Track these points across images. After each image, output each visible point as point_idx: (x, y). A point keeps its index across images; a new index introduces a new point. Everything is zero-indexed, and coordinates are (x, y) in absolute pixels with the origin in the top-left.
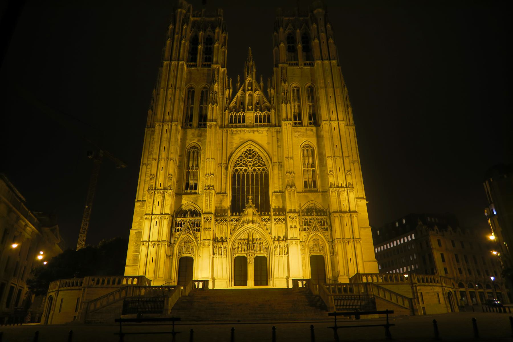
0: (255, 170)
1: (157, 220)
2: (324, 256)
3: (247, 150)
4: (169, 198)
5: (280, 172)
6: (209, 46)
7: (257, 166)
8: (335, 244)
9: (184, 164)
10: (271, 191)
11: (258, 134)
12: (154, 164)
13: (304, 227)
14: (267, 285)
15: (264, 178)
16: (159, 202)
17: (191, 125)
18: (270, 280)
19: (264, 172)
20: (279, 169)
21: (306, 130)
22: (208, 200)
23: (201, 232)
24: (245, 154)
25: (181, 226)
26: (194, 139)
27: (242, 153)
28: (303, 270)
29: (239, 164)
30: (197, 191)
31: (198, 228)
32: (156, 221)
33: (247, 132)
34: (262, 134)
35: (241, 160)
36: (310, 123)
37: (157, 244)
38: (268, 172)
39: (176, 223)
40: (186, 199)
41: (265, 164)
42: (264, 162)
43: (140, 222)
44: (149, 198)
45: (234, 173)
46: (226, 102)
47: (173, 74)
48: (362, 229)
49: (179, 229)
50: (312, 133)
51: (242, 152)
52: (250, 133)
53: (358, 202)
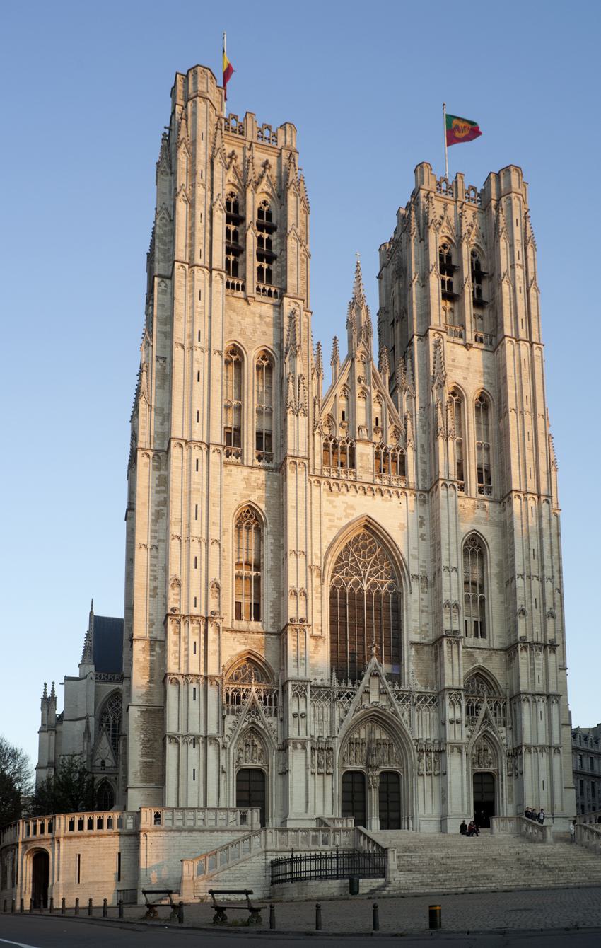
1: (195, 685)
3: (358, 535)
5: (423, 596)
8: (521, 753)
9: (231, 555)
11: (383, 500)
14: (399, 827)
17: (239, 455)
18: (408, 818)
25: (238, 703)
26: (249, 493)
38: (401, 593)
40: (242, 641)
46: (314, 407)
49: (236, 708)
51: (348, 541)
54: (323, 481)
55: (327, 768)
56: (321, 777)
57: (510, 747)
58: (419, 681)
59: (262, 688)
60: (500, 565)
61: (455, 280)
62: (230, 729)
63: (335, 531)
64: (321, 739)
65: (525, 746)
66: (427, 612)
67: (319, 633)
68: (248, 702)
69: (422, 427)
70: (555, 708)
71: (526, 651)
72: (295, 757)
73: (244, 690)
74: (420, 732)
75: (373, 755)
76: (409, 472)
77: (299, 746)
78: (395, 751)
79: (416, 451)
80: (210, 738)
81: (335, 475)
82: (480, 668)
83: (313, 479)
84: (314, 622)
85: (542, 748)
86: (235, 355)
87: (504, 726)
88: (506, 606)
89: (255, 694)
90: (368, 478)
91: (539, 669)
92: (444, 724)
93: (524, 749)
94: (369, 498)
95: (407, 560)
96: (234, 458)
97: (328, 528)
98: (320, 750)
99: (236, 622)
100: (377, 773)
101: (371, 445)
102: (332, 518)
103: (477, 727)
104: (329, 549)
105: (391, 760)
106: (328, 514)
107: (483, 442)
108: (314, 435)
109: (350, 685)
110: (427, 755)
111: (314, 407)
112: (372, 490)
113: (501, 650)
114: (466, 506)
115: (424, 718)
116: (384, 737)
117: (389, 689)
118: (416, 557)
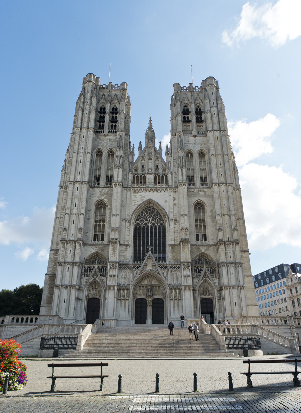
0: (154, 224)
2: (213, 300)
3: (147, 207)
4: (79, 247)
5: (175, 226)
6: (114, 115)
7: (156, 221)
10: (168, 242)
12: (67, 217)
13: (196, 274)
15: (162, 231)
16: (70, 250)
17: (98, 184)
19: (161, 227)
20: (174, 224)
21: (199, 190)
22: (113, 249)
23: (107, 278)
24: (145, 210)
25: (90, 272)
26: (101, 196)
27: (143, 210)
28: (195, 311)
29: (140, 219)
30: (103, 242)
31: (104, 273)
32: (68, 267)
33: (147, 191)
34: (161, 193)
35: (142, 215)
36: (202, 185)
37: (68, 288)
39: (85, 268)
40: (94, 248)
41: (162, 219)
42: (162, 217)
43: (54, 267)
44: (62, 247)
45: (136, 226)
46: (130, 165)
47: (83, 139)
48: (246, 277)
49: (88, 274)
50: (203, 193)
51: (143, 209)
52: (150, 192)
53: (242, 254)
54: (132, 189)
55: (126, 297)
56: (123, 301)
57: (218, 286)
58: (173, 260)
59: (100, 266)
60: (212, 211)
61: (190, 116)
62: (85, 282)
63: (136, 206)
64: (123, 285)
65: (224, 286)
66: (177, 232)
67: (128, 243)
68: (93, 271)
69: (175, 166)
70: (240, 269)
71: (223, 245)
72: (110, 293)
73: (92, 267)
74: (172, 281)
75: (149, 291)
76: (169, 182)
77: (112, 288)
78: (161, 289)
79: (172, 174)
80: (73, 286)
81: (137, 187)
82: (203, 253)
83: (127, 189)
84: (126, 239)
85: (234, 287)
86: (100, 152)
87: (216, 277)
88: (215, 227)
89: (97, 268)
90: (151, 186)
91: (230, 252)
92: (181, 277)
93: (223, 287)
94: (151, 193)
95: (167, 213)
96: (97, 185)
97: (133, 205)
98: (123, 290)
99: (93, 242)
100: (151, 299)
101: (153, 175)
102: (135, 201)
103: (201, 278)
104: (133, 212)
105: (159, 293)
106: (133, 200)
107: (203, 168)
108: (128, 174)
109: (139, 263)
110: (175, 291)
111: (130, 165)
112: (153, 190)
113: (214, 245)
114: (195, 191)
115: (174, 275)
116: (156, 283)
117: (156, 264)
118: (172, 212)
